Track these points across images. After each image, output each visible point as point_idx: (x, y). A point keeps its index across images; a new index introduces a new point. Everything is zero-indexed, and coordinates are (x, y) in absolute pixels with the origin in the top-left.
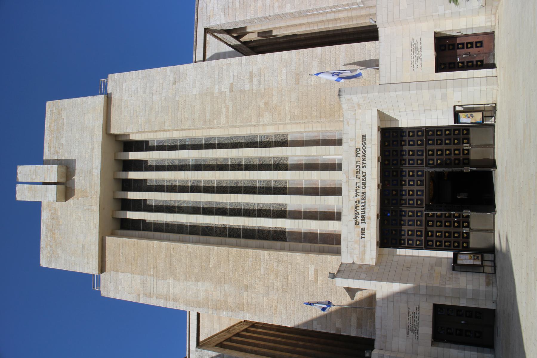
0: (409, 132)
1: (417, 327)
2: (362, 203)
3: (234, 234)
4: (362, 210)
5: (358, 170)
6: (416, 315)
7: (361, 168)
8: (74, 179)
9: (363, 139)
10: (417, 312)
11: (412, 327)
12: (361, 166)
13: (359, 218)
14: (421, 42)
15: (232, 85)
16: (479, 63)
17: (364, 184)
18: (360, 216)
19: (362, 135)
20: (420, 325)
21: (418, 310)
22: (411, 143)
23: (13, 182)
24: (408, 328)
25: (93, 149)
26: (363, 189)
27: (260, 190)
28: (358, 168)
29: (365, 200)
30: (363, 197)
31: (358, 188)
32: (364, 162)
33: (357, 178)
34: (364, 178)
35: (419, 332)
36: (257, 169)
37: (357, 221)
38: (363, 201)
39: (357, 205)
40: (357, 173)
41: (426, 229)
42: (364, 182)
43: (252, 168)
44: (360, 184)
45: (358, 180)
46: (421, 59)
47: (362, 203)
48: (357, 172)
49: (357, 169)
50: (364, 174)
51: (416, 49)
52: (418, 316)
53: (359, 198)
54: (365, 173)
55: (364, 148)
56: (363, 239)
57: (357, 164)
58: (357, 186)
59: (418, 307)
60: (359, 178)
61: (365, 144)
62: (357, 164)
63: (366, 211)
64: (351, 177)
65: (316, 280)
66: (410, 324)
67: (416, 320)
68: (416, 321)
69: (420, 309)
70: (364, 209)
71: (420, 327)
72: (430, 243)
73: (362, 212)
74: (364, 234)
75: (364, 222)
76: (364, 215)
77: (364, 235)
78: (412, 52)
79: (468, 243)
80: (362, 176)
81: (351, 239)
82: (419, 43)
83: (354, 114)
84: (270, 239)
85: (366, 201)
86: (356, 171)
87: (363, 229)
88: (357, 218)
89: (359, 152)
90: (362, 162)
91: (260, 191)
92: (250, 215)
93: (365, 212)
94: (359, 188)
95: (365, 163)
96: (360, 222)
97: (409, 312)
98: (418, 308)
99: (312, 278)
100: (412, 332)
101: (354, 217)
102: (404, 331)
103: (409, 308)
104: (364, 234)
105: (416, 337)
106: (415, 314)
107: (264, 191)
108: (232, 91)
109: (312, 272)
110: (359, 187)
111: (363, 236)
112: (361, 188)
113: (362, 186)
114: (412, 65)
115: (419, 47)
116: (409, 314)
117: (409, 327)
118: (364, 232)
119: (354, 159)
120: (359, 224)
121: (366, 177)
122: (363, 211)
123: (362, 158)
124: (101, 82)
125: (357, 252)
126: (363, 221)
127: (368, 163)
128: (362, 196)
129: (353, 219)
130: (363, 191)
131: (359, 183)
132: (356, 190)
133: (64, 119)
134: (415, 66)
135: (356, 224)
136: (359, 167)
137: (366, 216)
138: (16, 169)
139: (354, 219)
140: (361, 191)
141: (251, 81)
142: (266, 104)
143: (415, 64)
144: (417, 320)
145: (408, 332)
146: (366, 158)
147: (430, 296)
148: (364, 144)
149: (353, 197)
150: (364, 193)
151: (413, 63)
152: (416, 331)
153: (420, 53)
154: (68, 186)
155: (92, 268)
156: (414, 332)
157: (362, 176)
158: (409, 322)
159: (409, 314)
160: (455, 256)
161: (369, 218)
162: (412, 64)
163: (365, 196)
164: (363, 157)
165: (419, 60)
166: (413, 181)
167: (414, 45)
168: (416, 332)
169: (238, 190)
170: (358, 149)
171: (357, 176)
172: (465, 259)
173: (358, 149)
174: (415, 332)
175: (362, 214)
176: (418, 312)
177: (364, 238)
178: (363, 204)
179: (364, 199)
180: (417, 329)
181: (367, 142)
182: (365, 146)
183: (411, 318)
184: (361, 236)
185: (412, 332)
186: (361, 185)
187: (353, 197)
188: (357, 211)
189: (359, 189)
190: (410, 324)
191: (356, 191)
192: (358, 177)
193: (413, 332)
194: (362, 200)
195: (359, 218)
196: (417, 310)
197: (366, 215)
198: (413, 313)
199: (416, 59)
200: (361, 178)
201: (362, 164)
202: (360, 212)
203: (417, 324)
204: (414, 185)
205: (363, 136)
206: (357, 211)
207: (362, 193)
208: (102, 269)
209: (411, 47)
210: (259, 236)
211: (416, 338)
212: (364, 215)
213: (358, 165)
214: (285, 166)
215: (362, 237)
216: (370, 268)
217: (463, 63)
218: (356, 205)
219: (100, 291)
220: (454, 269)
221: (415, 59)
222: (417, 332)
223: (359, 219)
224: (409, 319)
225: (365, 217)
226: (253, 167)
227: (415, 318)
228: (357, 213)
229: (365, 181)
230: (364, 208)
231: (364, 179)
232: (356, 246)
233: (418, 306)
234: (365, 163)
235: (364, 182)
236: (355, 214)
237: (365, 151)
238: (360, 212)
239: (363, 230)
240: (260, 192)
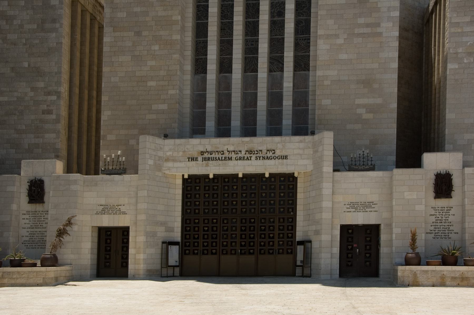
0: (293, 200)
1: (108, 213)
2: (222, 158)
3: (201, 12)
4: (215, 158)
5: (253, 152)
6: (118, 212)
7: (255, 155)
9: (284, 156)
10: (121, 212)
11: (107, 209)
12: (258, 155)
13: (208, 155)
14: (372, 211)
17: (240, 159)
19: (287, 156)
20: (109, 215)
21: (123, 213)
22: (282, 202)
24: (106, 205)
26: (234, 159)
27: (250, 41)
28: (256, 152)
29: (225, 160)
30: (227, 159)
31: (236, 152)
32: (261, 158)
33: (246, 151)
34: (246, 158)
35: (103, 215)
36: (274, 36)
37: (204, 153)
38: (223, 158)
39: (219, 153)
40: (250, 152)
42: (242, 159)
43: (274, 30)
44: (240, 155)
45: (243, 153)
46: (355, 212)
47: (222, 158)
48: (252, 152)
49: (254, 151)
50: (249, 158)
51: (365, 207)
52: (118, 213)
53: (227, 155)
54: (251, 160)
55: (275, 158)
56: (188, 160)
57: (260, 151)
58: (238, 152)
59: (125, 213)
60: (246, 154)
61: (279, 158)
62: (260, 151)
63: (214, 162)
64: (247, 146)
66: (110, 207)
67: (114, 212)
68: (113, 212)
69: (124, 215)
70: (215, 160)
71: (107, 215)
73: (213, 158)
74: (193, 160)
75: (204, 160)
76: (210, 159)
77: (191, 161)
78: (363, 203)
80: (247, 157)
81: (187, 148)
82: (371, 209)
83: (309, 147)
84: (197, 56)
85: (224, 162)
86: (253, 151)
87: (196, 159)
88: (207, 153)
89: (271, 153)
90: (261, 157)
91: (249, 41)
92: (223, 31)
93: (213, 160)
94: (236, 154)
95: (260, 159)
96: (204, 156)
97: (120, 205)
98: (124, 213)
99: (154, 107)
100: (103, 209)
101: (209, 150)
102: (103, 202)
103: (124, 205)
104: (193, 160)
105: (98, 213)
106: (119, 211)
107: (249, 46)
110: (237, 153)
111: (190, 160)
112: (236, 156)
113: (238, 157)
114: (349, 204)
115: (367, 210)
116: (119, 205)
117: (107, 206)
118: (194, 161)
119: (264, 148)
120: (202, 155)
121: (246, 160)
122: (214, 159)
123: (265, 156)
125: (175, 154)
126: (205, 159)
127: (260, 162)
128: (229, 158)
129: (206, 149)
131: (241, 154)
132: (234, 151)
134: (348, 206)
135: (201, 152)
136: (257, 154)
137: (209, 162)
139: (206, 150)
140: (234, 156)
143: (350, 206)
144: (114, 213)
145: (103, 205)
146: (265, 159)
148: (279, 157)
149: (227, 149)
150: (230, 159)
151: (352, 204)
152: (104, 212)
153: (361, 211)
156: (103, 211)
157: (247, 157)
158: (112, 206)
159: (119, 205)
161: (207, 165)
162: (351, 203)
163: (228, 160)
164: (266, 157)
165: (354, 210)
166: (246, 205)
167: (369, 205)
168: (103, 212)
169: (250, 14)
170: (273, 152)
171: (248, 151)
173: (273, 152)
174: (103, 212)
175: (211, 158)
176: (122, 213)
177: (189, 161)
178: (220, 159)
179: (226, 159)
180: (106, 213)
181: (280, 161)
182: (277, 159)
183: (115, 207)
184: (190, 158)
185: (103, 209)
187: (227, 149)
188: (214, 153)
189: (235, 154)
190: (110, 207)
191: (233, 151)
192: (247, 153)
193: (103, 210)
194: (225, 157)
195: (208, 155)
196: (123, 212)
197: (211, 162)
198: (120, 209)
199: (356, 207)
200: (246, 156)
201: (259, 157)
202: (213, 155)
203: (110, 213)
205: (286, 157)
206: (214, 153)
207: (231, 158)
209: (368, 203)
210: (200, 43)
211: (97, 213)
212: (210, 159)
213: (259, 152)
214: (275, 70)
215: (189, 158)
218: (220, 152)
221: (356, 206)
222: (103, 213)
223: (206, 155)
224: (114, 205)
225: (208, 160)
226: (275, 31)
227: (115, 211)
228: (212, 153)
229: (243, 160)
230: (217, 159)
231: (245, 158)
232: (181, 153)
233: (126, 214)
234: (260, 159)
235: (242, 159)
236: (211, 151)
237: (272, 158)
238: (213, 155)
239: (196, 159)
240: (247, 41)
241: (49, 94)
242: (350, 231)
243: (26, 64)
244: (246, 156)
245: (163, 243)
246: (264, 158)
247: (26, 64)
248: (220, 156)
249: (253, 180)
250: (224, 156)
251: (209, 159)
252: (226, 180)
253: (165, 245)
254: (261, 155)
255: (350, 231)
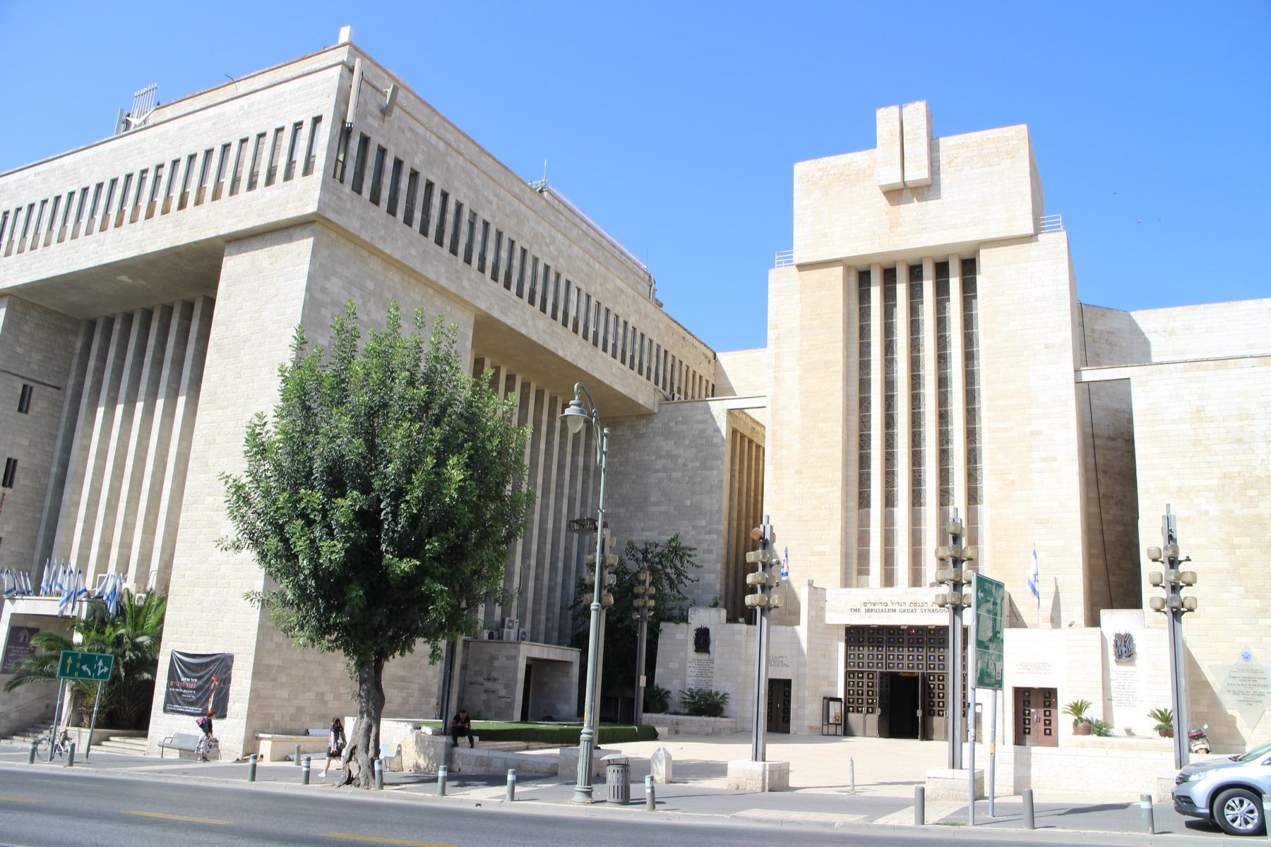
8: (913, 202)
15: (1039, 433)
16: (1027, 731)
18: (872, 607)
23: (901, 101)
25: (956, 228)
41: (865, 671)
45: (908, 604)
53: (890, 607)
65: (813, 554)
72: (852, 676)
79: (853, 711)
108: (1032, 433)
109: (823, 548)
124: (1059, 217)
127: (927, 615)
130: (897, 610)
133: (999, 164)
138: (919, 99)
140: (897, 607)
141: (1044, 460)
142: (1013, 482)
147: (798, 677)
154: (904, 192)
155: (802, 253)
160: (840, 700)
161: (870, 617)
166: (913, 660)
172: (835, 709)
186: (903, 608)
197: (873, 613)
202: (876, 607)
204: (908, 660)
208: (801, 267)
216: (822, 619)
217: (1029, 714)
219: (774, 267)
220: (824, 698)
223: (869, 607)
238: (876, 607)
241: (710, 532)
242: (1027, 694)
243: (688, 502)
244: (910, 608)
245: (824, 698)
246: (929, 611)
247: (688, 502)
248: (884, 608)
249: (920, 632)
250: (887, 608)
251: (872, 610)
252: (892, 632)
253: (826, 701)
254: (926, 608)
255: (1027, 694)
